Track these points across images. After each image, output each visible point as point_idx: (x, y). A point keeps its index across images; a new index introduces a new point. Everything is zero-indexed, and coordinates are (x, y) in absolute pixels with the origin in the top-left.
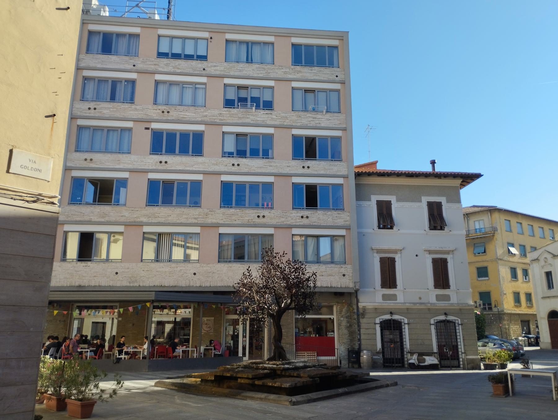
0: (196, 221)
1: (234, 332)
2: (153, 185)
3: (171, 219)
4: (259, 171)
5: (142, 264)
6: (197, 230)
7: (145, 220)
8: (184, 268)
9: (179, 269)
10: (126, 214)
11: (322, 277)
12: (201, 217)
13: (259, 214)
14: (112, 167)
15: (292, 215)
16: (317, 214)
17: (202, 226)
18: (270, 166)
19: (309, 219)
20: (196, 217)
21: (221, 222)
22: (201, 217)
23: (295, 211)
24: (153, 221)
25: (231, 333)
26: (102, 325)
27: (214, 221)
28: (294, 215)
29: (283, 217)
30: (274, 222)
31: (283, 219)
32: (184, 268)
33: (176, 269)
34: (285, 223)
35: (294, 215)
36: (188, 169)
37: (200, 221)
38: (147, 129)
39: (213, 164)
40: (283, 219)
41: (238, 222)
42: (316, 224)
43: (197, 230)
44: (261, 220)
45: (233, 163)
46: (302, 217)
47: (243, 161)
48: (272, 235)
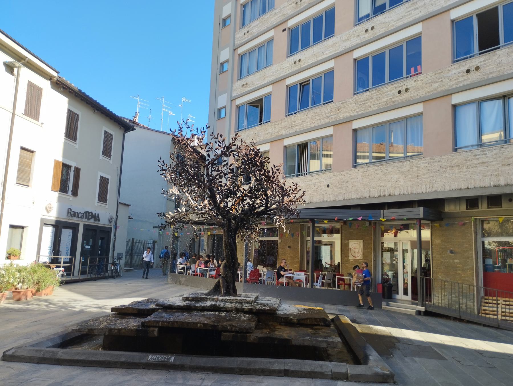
0: (327, 121)
1: (392, 260)
3: (308, 124)
4: (400, 23)
6: (329, 131)
7: (284, 132)
8: (318, 181)
9: (314, 181)
10: (270, 130)
11: (507, 168)
12: (333, 113)
13: (400, 89)
14: (260, 85)
15: (450, 74)
16: (495, 58)
17: (335, 125)
18: (415, 9)
19: (481, 70)
20: (327, 115)
21: (354, 114)
22: (333, 113)
23: (456, 65)
24: (291, 132)
25: (389, 261)
27: (347, 115)
28: (454, 71)
29: (436, 82)
30: (422, 93)
31: (436, 85)
32: (318, 181)
33: (311, 182)
34: (439, 89)
35: (454, 71)
36: (319, 58)
37: (333, 119)
38: (284, 30)
39: (345, 41)
40: (436, 85)
41: (374, 108)
42: (494, 75)
43: (329, 131)
44: (405, 96)
45: (366, 28)
46: (468, 71)
47: (381, 18)
48: (421, 114)
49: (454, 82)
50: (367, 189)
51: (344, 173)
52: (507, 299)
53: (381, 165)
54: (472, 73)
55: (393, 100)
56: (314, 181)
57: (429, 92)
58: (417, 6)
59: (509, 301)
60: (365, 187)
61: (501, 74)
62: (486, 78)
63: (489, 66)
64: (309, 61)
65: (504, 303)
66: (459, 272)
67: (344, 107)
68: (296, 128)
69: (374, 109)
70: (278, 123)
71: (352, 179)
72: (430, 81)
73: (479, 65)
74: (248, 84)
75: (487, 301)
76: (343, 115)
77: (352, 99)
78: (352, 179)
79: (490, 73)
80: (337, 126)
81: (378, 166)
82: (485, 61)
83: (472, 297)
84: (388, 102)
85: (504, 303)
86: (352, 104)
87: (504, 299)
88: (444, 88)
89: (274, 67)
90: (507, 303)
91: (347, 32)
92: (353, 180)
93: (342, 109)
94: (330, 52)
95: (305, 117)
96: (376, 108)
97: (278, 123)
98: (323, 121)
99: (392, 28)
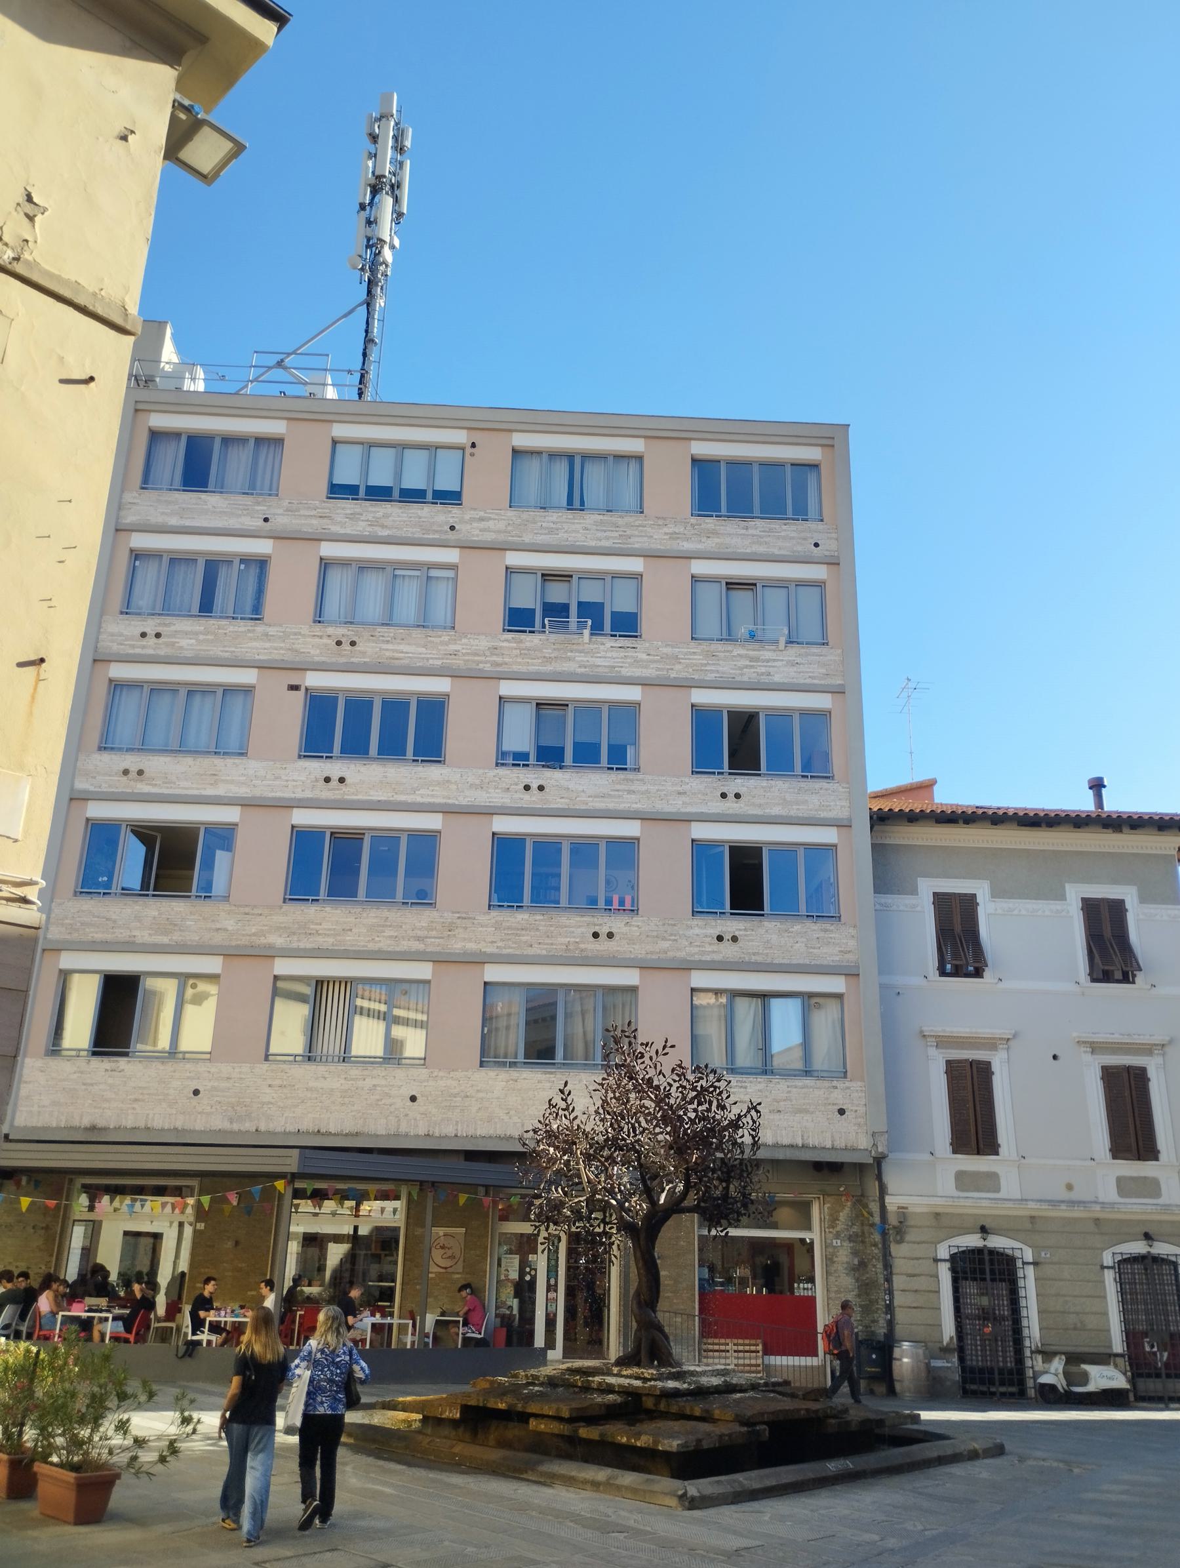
0: (419, 946)
1: (522, 1273)
2: (305, 842)
3: (357, 938)
4: (600, 805)
5: (266, 1066)
6: (424, 971)
7: (278, 941)
8: (383, 1082)
9: (369, 1082)
10: (230, 924)
11: (776, 1116)
12: (434, 933)
13: (597, 929)
14: (196, 792)
15: (690, 933)
16: (762, 931)
17: (440, 960)
18: (630, 792)
19: (740, 943)
20: (419, 933)
21: (490, 949)
22: (434, 933)
23: (699, 921)
24: (302, 945)
25: (514, 1275)
26: (151, 1240)
27: (471, 946)
28: (697, 931)
29: (664, 939)
30: (639, 951)
31: (666, 945)
32: (383, 1082)
33: (360, 1083)
34: (671, 954)
35: (697, 931)
36: (402, 798)
37: (433, 945)
38: (294, 688)
39: (472, 786)
40: (666, 945)
41: (536, 950)
42: (759, 959)
43: (424, 971)
44: (603, 945)
45: (527, 781)
46: (720, 938)
47: (553, 777)
48: (633, 990)
49: (697, 949)
50: (515, 1119)
51: (459, 1074)
52: (740, 1341)
53: (551, 1073)
54: (725, 943)
55: (582, 946)
56: (369, 1082)
57: (652, 953)
58: (633, 788)
59: (750, 1345)
60: (512, 1112)
61: (769, 961)
62: (747, 959)
63: (752, 941)
64: (372, 793)
65: (735, 1348)
66: (669, 1294)
67: (466, 928)
68: (320, 939)
69: (539, 952)
70: (256, 911)
71: (478, 1091)
72: (655, 934)
73: (737, 934)
74: (146, 774)
75: (711, 1347)
76: (459, 944)
77: (487, 917)
78: (478, 1091)
79: (754, 954)
80: (443, 966)
81: (546, 1073)
82: (745, 930)
83: (691, 1342)
84: (571, 947)
85: (735, 1348)
86: (486, 926)
87: (735, 1341)
88: (681, 954)
89: (252, 766)
90: (741, 1348)
91: (481, 771)
92: (481, 1095)
93: (461, 930)
94: (432, 796)
95: (352, 919)
96: (544, 952)
97: (256, 911)
98: (405, 943)
99: (584, 807)
